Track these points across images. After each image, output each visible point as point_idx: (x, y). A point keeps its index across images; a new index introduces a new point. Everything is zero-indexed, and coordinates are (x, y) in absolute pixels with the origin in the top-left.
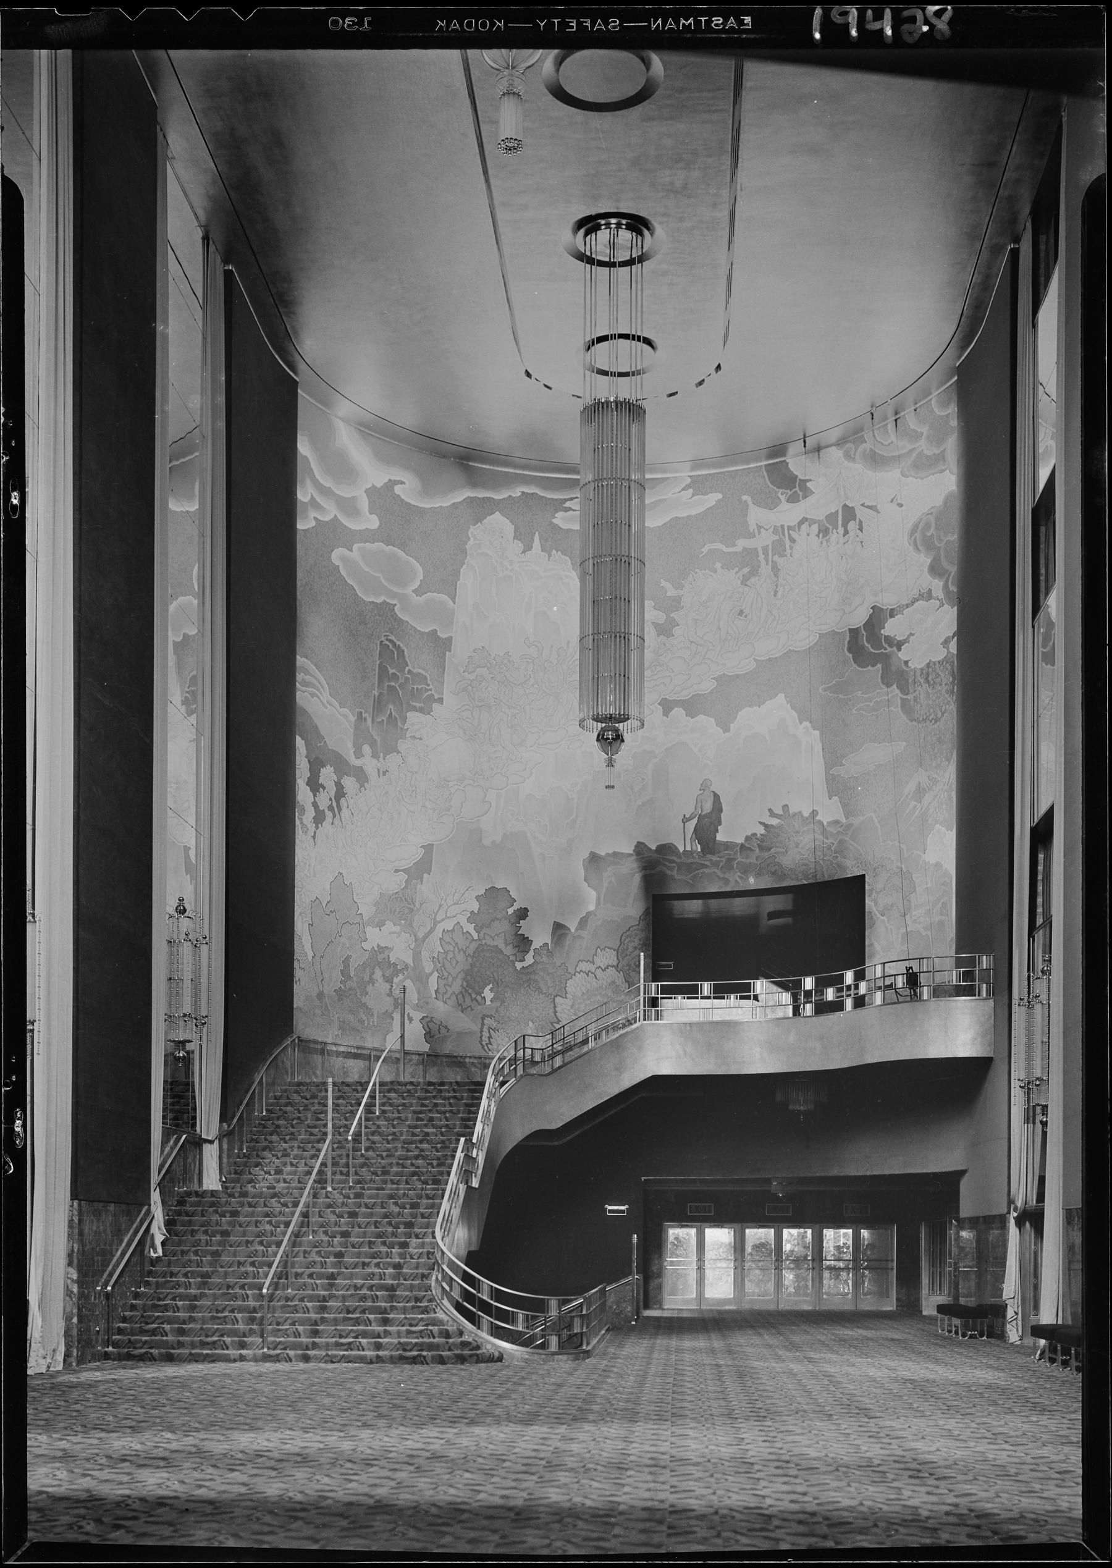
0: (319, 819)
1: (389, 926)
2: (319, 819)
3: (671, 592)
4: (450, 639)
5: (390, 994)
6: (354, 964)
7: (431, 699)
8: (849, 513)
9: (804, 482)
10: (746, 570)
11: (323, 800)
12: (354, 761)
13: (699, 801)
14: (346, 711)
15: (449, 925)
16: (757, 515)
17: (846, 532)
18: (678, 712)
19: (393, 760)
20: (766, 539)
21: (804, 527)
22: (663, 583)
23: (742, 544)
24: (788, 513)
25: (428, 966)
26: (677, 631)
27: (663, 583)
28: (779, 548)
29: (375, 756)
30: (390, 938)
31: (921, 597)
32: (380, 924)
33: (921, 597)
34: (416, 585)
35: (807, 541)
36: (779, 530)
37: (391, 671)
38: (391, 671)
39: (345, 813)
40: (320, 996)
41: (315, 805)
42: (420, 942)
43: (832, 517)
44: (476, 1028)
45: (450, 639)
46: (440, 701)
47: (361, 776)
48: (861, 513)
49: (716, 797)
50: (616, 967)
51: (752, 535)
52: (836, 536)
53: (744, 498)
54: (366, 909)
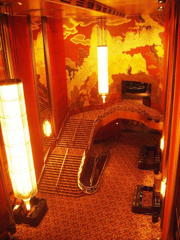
0: (71, 79)
1: (83, 90)
2: (71, 79)
3: (124, 35)
4: (90, 46)
5: (84, 99)
6: (78, 97)
7: (88, 55)
8: (150, 27)
9: (144, 20)
10: (135, 32)
11: (71, 77)
12: (76, 69)
13: (128, 68)
14: (74, 62)
15: (92, 87)
16: (137, 24)
17: (150, 30)
18: (125, 53)
19: (82, 66)
20: (138, 28)
21: (144, 27)
22: (123, 33)
24: (141, 24)
25: (89, 93)
26: (125, 41)
27: (123, 33)
28: (140, 29)
29: (79, 66)
30: (84, 92)
31: (160, 45)
32: (81, 90)
33: (160, 45)
34: (84, 39)
35: (144, 29)
36: (140, 27)
37: (81, 53)
38: (81, 53)
39: (75, 77)
40: (73, 103)
41: (70, 78)
42: (87, 91)
43: (148, 26)
44: (96, 101)
45: (90, 46)
46: (89, 55)
47: (77, 70)
48: (152, 27)
49: (131, 67)
50: (117, 91)
51: (136, 27)
52: (149, 30)
53: (135, 20)
54: (79, 89)
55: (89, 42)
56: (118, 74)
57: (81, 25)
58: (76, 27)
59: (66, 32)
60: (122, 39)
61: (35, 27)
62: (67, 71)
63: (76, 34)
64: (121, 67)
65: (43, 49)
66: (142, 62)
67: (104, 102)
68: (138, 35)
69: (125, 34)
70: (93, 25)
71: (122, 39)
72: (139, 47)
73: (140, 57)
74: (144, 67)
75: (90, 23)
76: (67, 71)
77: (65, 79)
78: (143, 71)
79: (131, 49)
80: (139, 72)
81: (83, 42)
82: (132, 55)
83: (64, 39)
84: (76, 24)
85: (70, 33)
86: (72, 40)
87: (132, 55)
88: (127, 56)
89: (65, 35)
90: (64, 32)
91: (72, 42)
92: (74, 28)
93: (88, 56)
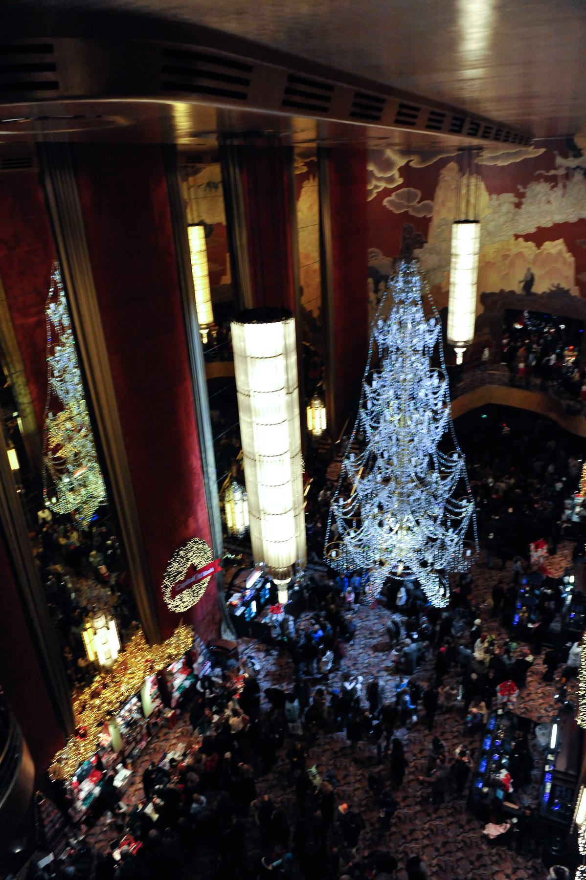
11: (380, 294)
13: (526, 277)
16: (559, 160)
18: (521, 240)
20: (561, 172)
23: (552, 172)
24: (572, 162)
26: (523, 206)
28: (567, 176)
36: (568, 168)
51: (555, 169)
55: (430, 209)
56: (497, 291)
57: (411, 164)
58: (400, 169)
59: (374, 183)
60: (516, 200)
61: (300, 167)
62: (370, 280)
63: (399, 187)
64: (507, 274)
65: (317, 227)
66: (565, 262)
67: (459, 361)
68: (558, 191)
69: (525, 188)
70: (443, 163)
71: (516, 200)
72: (558, 224)
73: (561, 250)
74: (567, 277)
75: (436, 160)
76: (370, 280)
77: (366, 300)
78: (565, 285)
79: (539, 228)
80: (554, 289)
81: (413, 207)
82: (539, 245)
83: (370, 199)
84: (401, 162)
85: (383, 185)
86: (389, 202)
87: (539, 245)
88: (526, 247)
89: (371, 191)
90: (370, 182)
91: (388, 207)
92: (395, 173)
93: (426, 245)
